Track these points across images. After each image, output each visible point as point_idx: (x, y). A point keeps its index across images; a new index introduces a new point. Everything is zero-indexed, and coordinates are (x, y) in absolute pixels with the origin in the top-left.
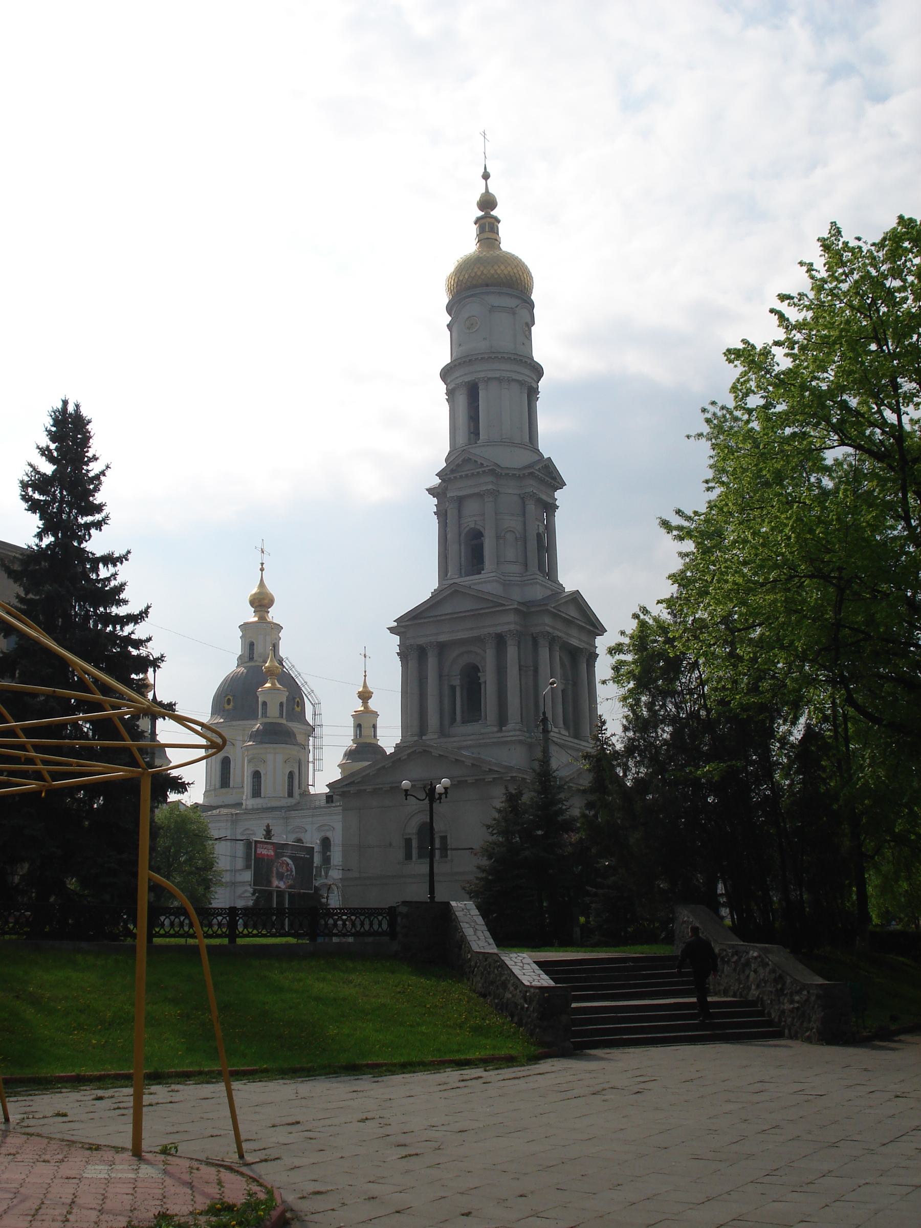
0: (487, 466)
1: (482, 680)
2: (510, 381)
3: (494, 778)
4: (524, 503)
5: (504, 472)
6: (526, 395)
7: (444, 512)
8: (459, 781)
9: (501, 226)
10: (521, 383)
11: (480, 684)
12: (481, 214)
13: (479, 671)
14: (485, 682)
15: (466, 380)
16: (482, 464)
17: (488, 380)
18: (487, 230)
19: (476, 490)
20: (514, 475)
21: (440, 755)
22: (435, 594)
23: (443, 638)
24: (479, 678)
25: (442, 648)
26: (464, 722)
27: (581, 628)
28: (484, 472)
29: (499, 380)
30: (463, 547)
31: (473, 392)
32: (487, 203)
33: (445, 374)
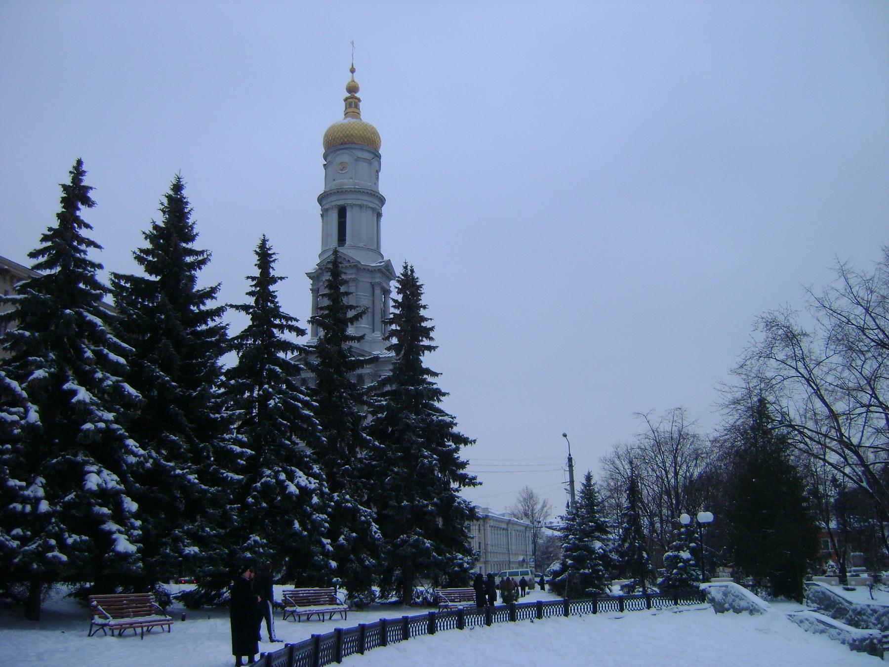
0: (353, 262)
2: (368, 207)
4: (373, 288)
6: (376, 217)
7: (317, 289)
9: (361, 104)
10: (373, 210)
12: (348, 95)
15: (338, 204)
16: (349, 261)
17: (353, 206)
18: (353, 106)
20: (368, 270)
28: (350, 266)
29: (360, 206)
31: (342, 212)
32: (352, 89)
33: (321, 199)
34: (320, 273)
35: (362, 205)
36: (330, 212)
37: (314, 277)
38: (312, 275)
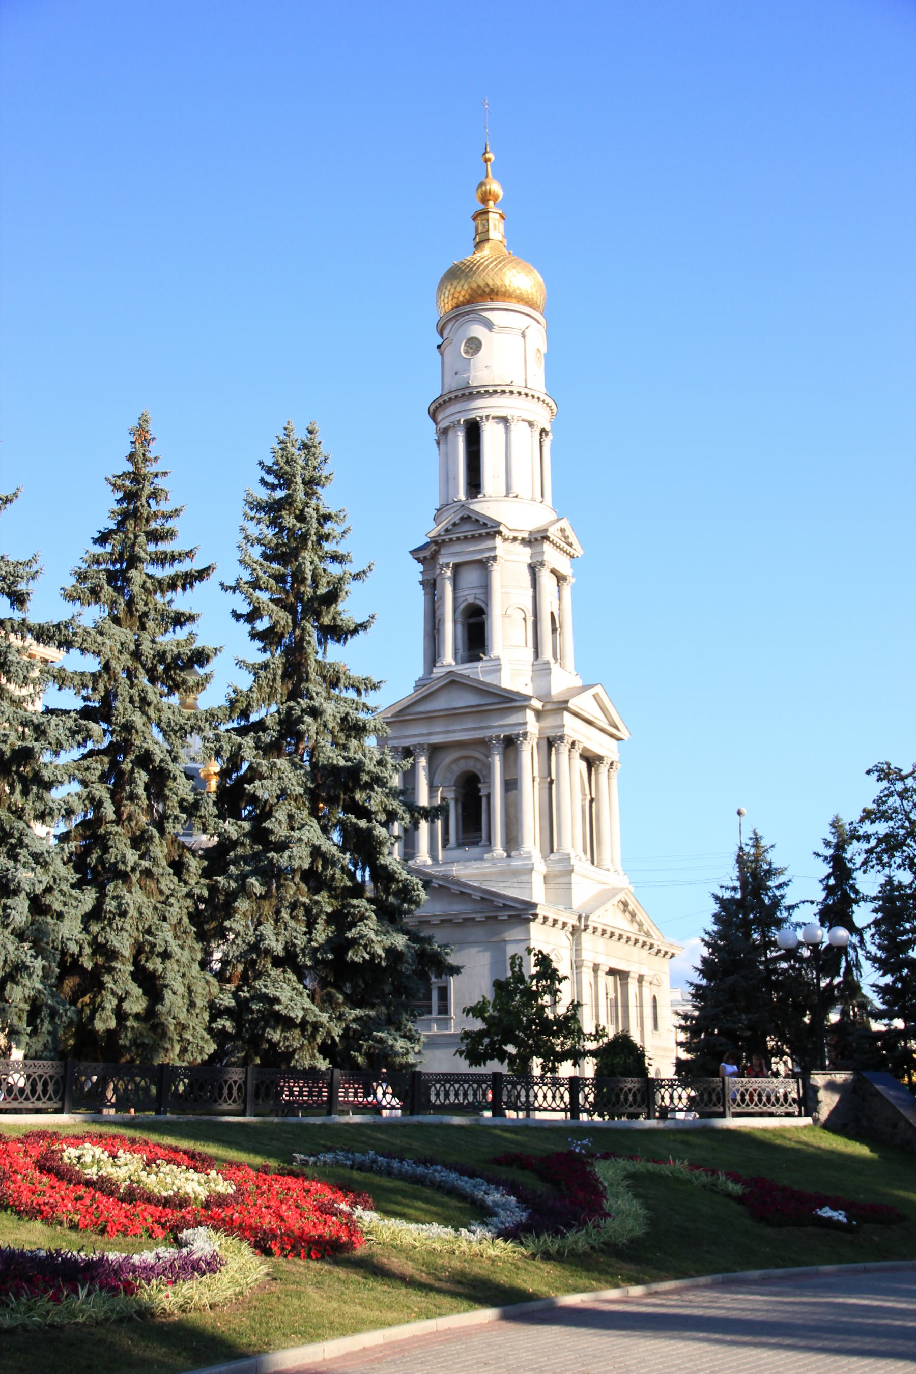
0: (492, 527)
1: (483, 793)
3: (510, 916)
5: (511, 535)
7: (432, 581)
8: (464, 919)
11: (480, 798)
13: (479, 781)
14: (489, 796)
16: (485, 524)
19: (479, 557)
20: (523, 540)
21: (440, 885)
22: (419, 685)
23: (436, 739)
24: (479, 790)
25: (434, 751)
26: (461, 845)
27: (602, 730)
28: (488, 534)
30: (459, 627)
34: (435, 550)
35: (509, 417)
36: (451, 434)
37: (425, 558)
38: (422, 555)
